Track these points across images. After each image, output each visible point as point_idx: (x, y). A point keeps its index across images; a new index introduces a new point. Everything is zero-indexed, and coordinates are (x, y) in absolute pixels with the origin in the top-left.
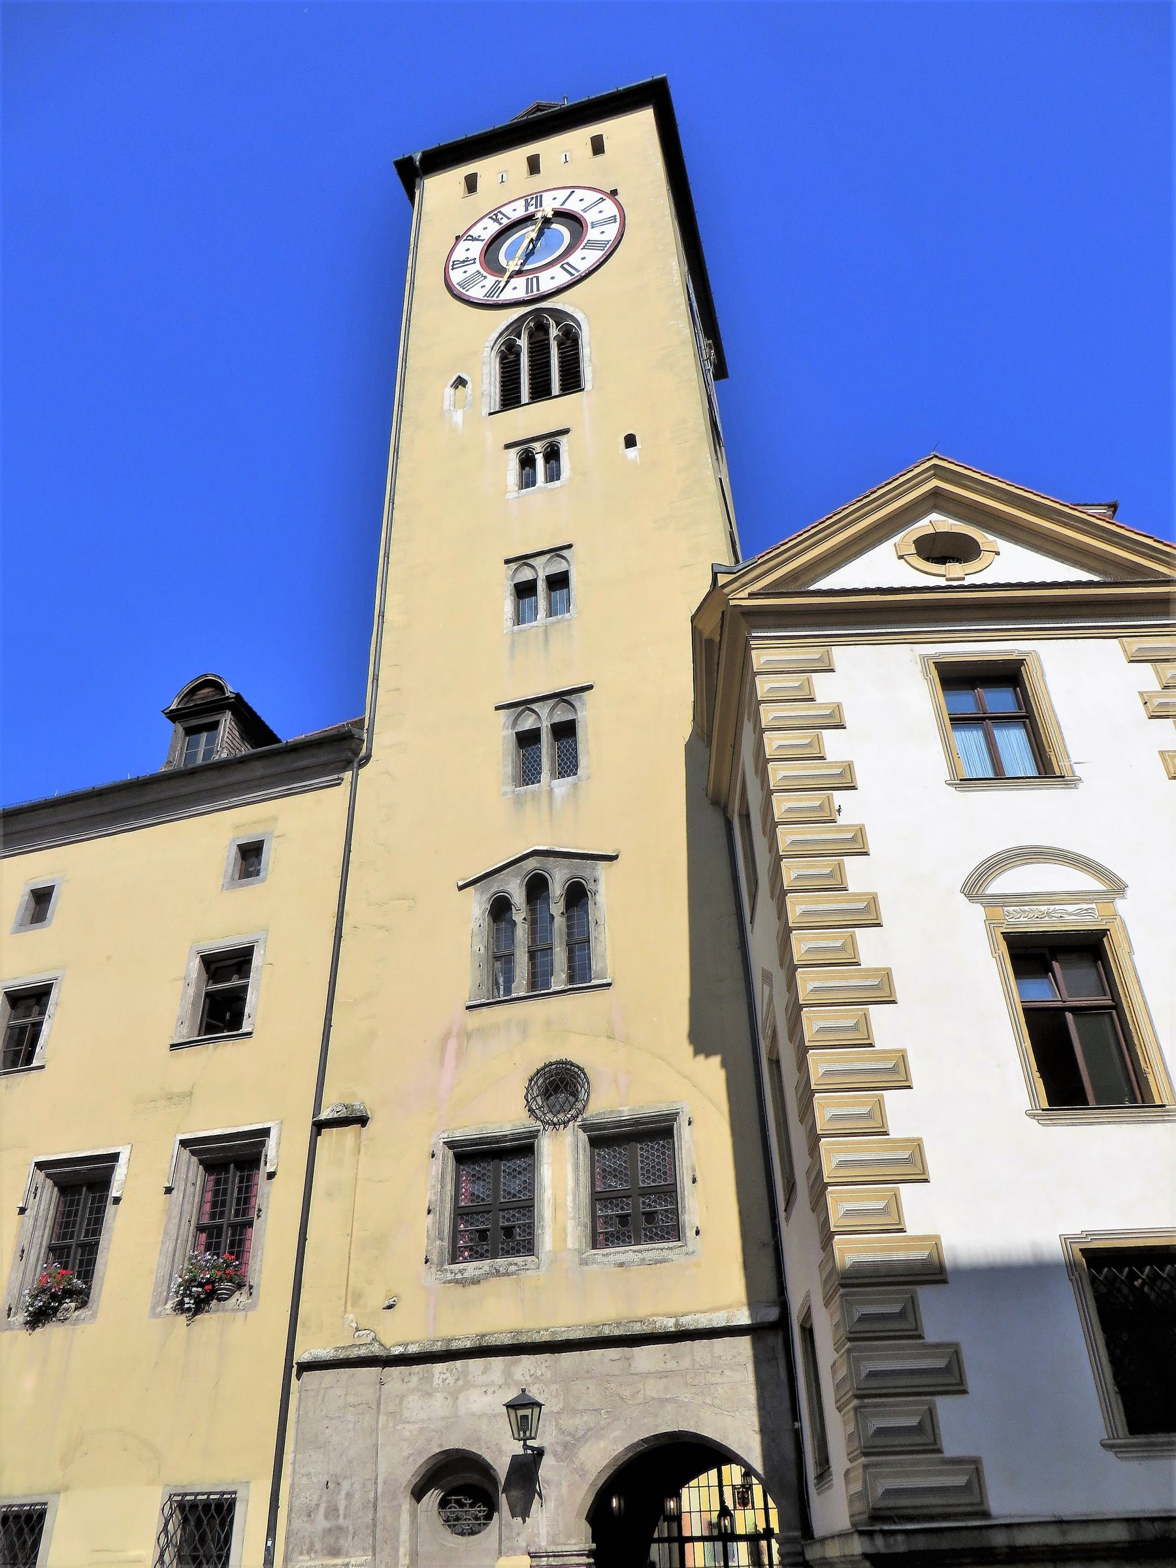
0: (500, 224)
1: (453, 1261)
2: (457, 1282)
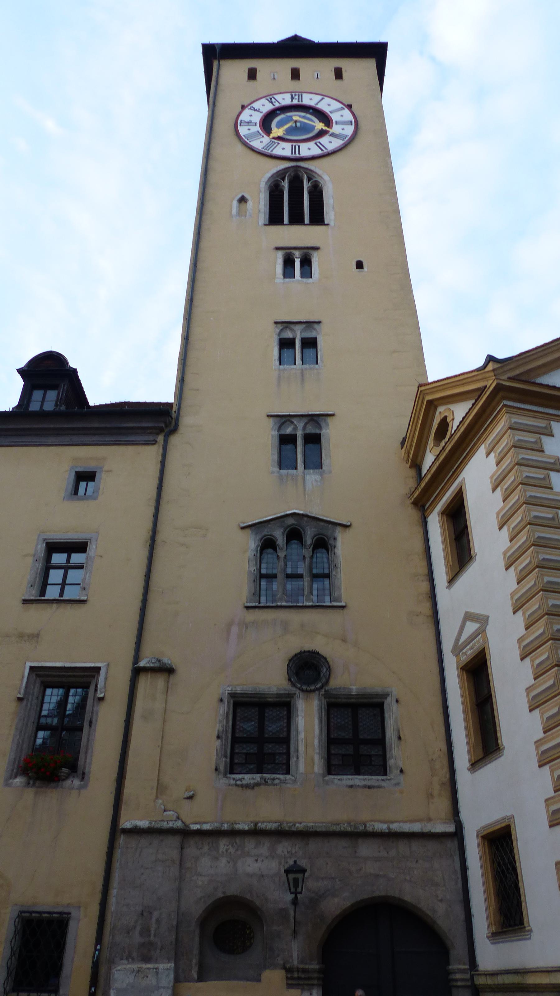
0: (273, 105)
1: (231, 772)
2: (237, 785)
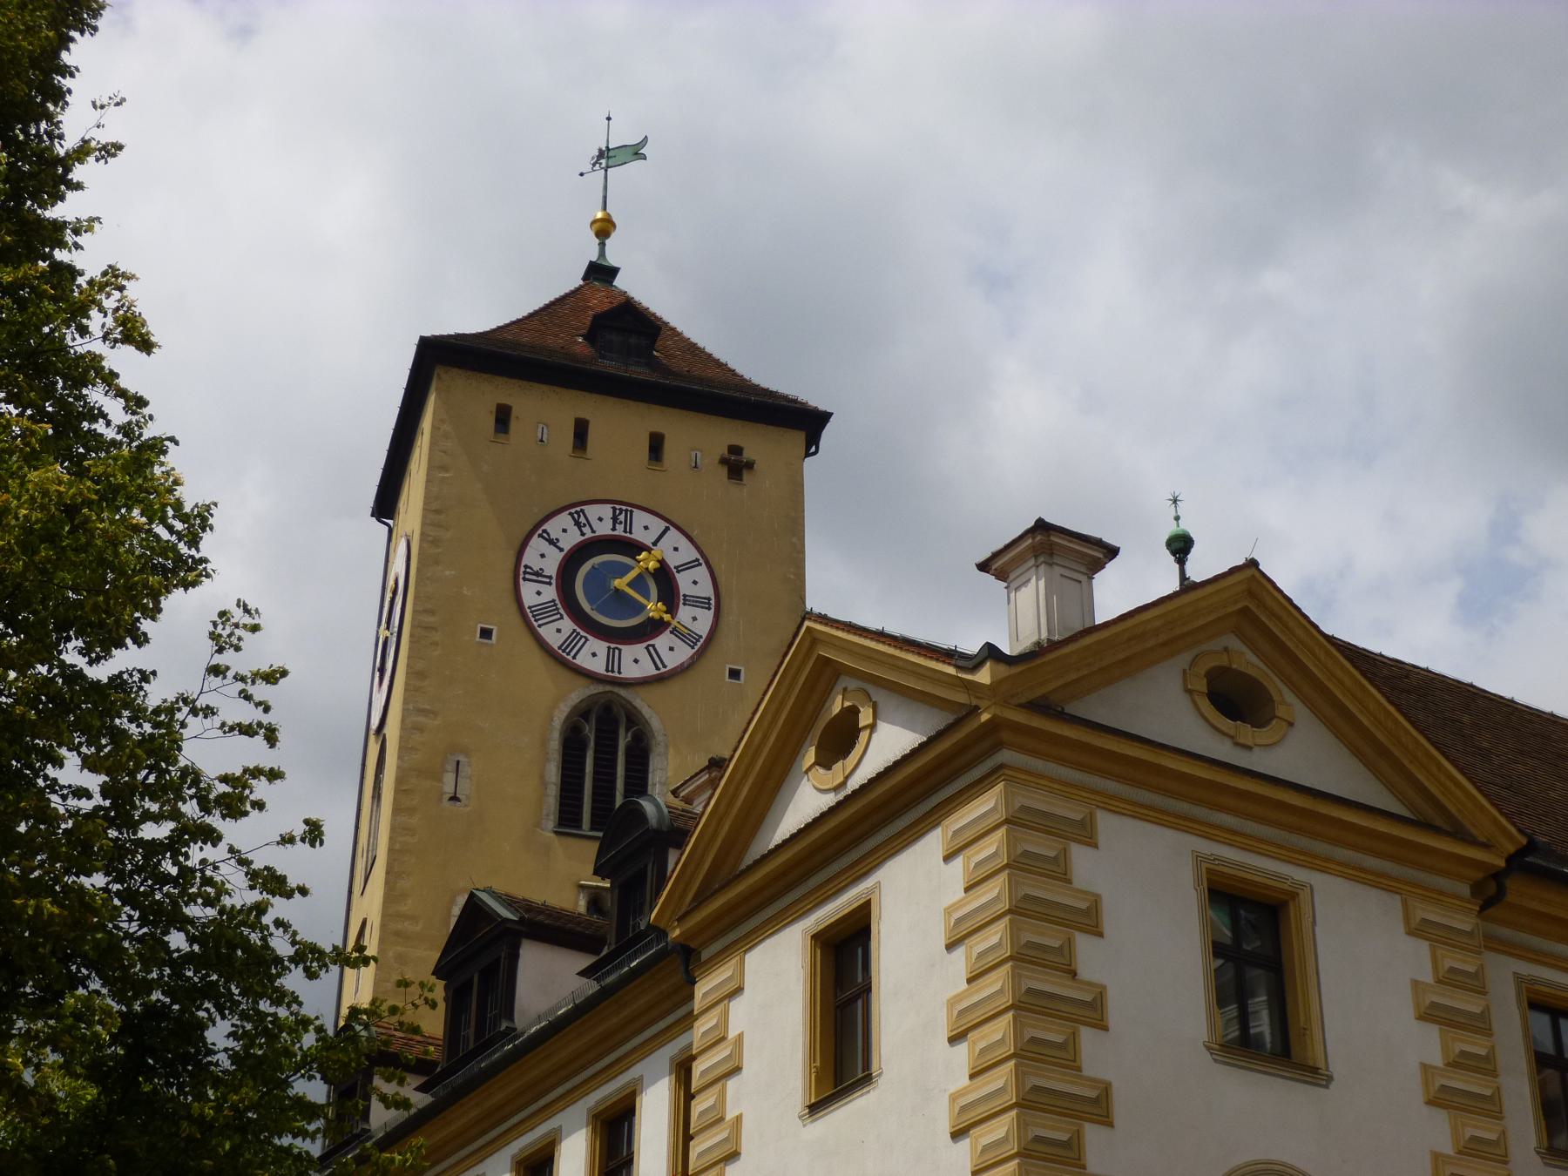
0: (583, 534)
